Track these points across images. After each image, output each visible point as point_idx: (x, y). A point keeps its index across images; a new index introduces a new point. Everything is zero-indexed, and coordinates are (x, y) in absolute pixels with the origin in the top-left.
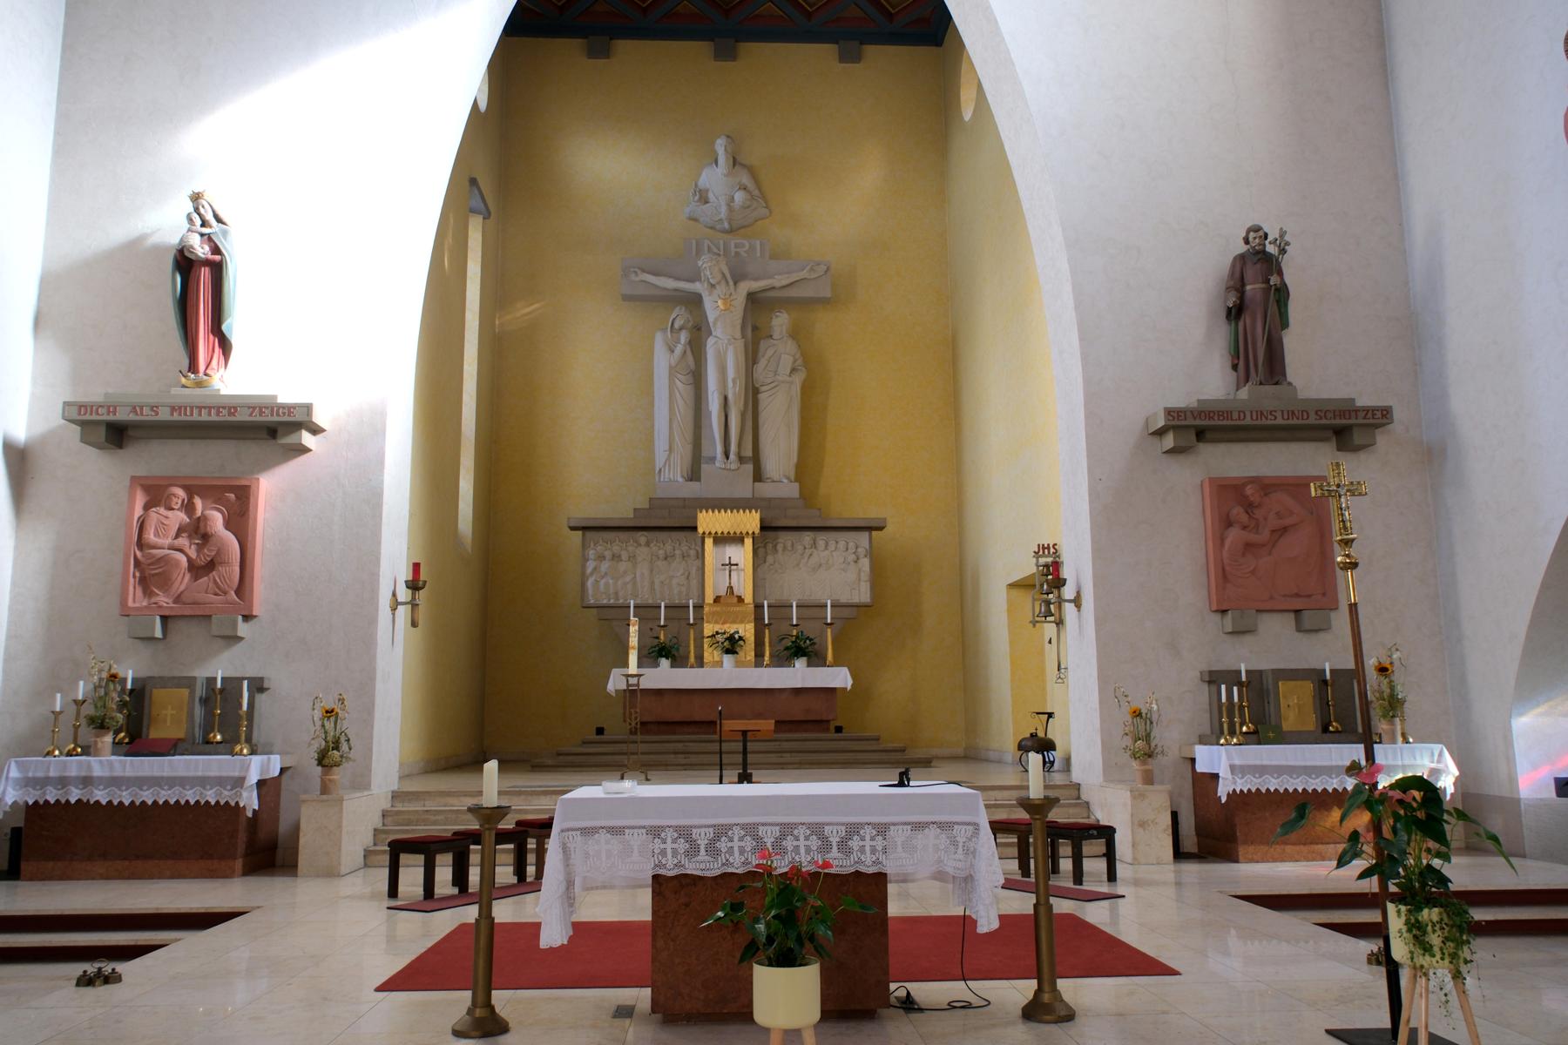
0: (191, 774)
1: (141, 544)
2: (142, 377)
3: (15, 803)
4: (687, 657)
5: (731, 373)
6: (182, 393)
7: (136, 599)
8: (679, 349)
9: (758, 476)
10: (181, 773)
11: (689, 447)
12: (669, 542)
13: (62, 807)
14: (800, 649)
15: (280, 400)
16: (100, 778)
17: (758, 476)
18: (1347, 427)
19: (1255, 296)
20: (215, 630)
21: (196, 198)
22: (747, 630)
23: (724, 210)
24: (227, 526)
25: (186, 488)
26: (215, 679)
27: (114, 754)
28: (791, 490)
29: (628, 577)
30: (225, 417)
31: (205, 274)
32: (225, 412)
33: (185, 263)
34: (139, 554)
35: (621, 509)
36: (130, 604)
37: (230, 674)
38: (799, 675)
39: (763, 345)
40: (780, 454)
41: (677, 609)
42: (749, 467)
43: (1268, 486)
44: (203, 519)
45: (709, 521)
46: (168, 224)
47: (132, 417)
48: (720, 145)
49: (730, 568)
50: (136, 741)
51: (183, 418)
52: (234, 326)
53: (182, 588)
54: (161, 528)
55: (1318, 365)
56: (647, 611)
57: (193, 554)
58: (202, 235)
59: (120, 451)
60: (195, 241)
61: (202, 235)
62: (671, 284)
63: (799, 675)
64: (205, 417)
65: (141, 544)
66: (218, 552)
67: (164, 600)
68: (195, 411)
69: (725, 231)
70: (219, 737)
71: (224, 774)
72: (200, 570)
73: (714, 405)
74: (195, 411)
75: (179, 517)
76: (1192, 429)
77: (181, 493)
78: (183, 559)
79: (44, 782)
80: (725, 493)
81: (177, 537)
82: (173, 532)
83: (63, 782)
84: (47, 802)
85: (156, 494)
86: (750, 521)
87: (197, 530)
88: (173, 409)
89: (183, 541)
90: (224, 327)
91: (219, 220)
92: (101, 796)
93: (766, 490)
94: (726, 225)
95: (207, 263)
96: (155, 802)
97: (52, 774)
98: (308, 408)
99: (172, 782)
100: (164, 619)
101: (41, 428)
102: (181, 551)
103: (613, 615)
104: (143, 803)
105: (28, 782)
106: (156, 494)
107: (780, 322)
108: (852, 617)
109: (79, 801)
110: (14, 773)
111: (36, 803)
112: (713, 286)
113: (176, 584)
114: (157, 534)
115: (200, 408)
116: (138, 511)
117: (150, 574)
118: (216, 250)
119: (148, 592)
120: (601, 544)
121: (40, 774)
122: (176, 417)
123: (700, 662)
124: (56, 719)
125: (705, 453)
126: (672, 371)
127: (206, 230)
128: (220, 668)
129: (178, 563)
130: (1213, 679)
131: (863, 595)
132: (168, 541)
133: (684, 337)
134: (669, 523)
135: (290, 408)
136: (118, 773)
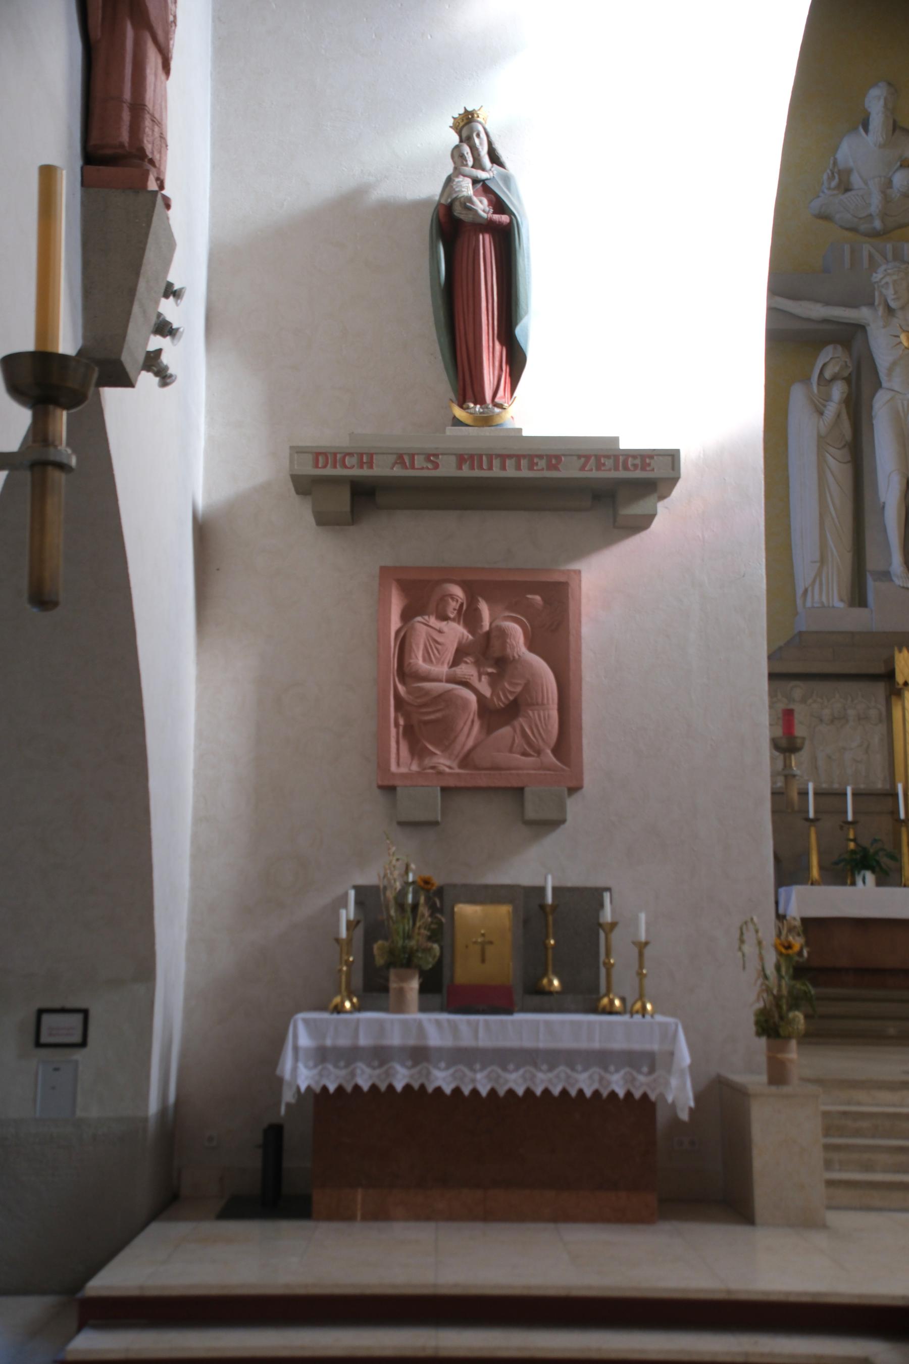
0: (583, 1045)
1: (405, 673)
2: (390, 406)
3: (309, 1088)
4: (808, 868)
6: (472, 437)
7: (401, 762)
8: (831, 409)
10: (567, 1043)
11: (848, 557)
13: (380, 1097)
15: (625, 445)
16: (440, 1050)
20: (531, 813)
21: (466, 124)
23: (876, 202)
24: (532, 646)
25: (465, 585)
26: (542, 890)
27: (423, 1009)
30: (541, 472)
31: (486, 244)
32: (542, 463)
34: (401, 688)
36: (394, 768)
37: (574, 879)
44: (498, 635)
46: (415, 162)
47: (398, 471)
51: (477, 473)
52: (534, 330)
53: (470, 743)
54: (433, 646)
57: (487, 691)
58: (475, 181)
59: (351, 528)
60: (466, 188)
61: (475, 181)
62: (817, 311)
64: (510, 472)
65: (405, 673)
66: (527, 687)
67: (444, 762)
68: (496, 463)
69: (875, 234)
70: (556, 983)
71: (637, 1046)
72: (494, 715)
74: (496, 463)
77: (458, 591)
78: (473, 698)
79: (350, 1055)
81: (455, 663)
82: (450, 656)
83: (380, 1055)
84: (357, 1088)
85: (419, 593)
87: (487, 651)
88: (461, 459)
89: (467, 670)
90: (518, 331)
91: (495, 158)
92: (442, 1079)
94: (878, 224)
95: (490, 227)
96: (529, 1092)
97: (364, 1041)
98: (673, 456)
99: (552, 1058)
100: (444, 789)
101: (225, 491)
102: (466, 684)
104: (511, 1092)
105: (322, 1055)
106: (419, 593)
109: (408, 1087)
110: (305, 1040)
111: (340, 1089)
112: (890, 311)
113: (462, 738)
114: (428, 658)
115: (503, 457)
116: (395, 622)
117: (421, 720)
118: (499, 206)
119: (417, 751)
121: (344, 1042)
122: (466, 472)
124: (641, 955)
125: (873, 562)
126: (822, 442)
127: (482, 175)
128: (541, 866)
129: (466, 702)
132: (443, 669)
133: (838, 391)
135: (645, 457)
136: (467, 1041)
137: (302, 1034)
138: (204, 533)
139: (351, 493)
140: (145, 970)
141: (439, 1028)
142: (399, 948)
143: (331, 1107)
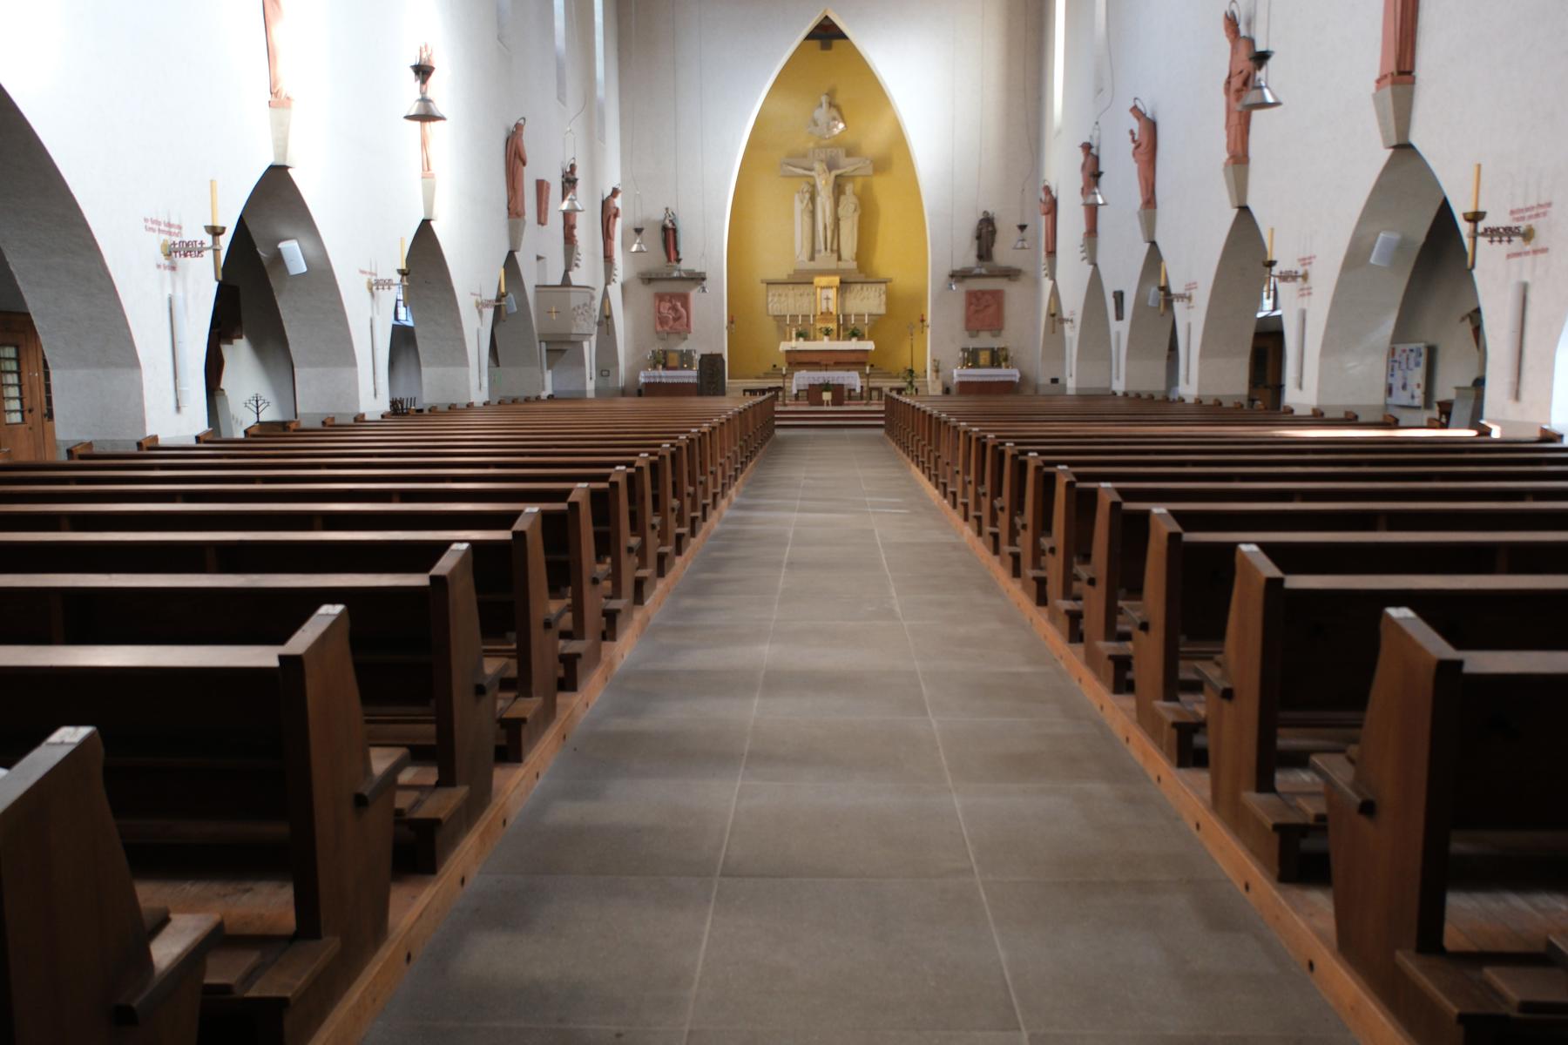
5: (828, 213)
9: (839, 258)
12: (802, 288)
14: (855, 334)
17: (839, 258)
18: (1011, 274)
19: (986, 232)
22: (833, 326)
28: (854, 265)
29: (788, 303)
33: (665, 229)
35: (782, 275)
38: (854, 344)
39: (842, 198)
40: (849, 246)
41: (806, 317)
42: (835, 256)
43: (984, 293)
45: (820, 281)
48: (824, 99)
49: (826, 297)
50: (665, 367)
55: (1004, 253)
56: (794, 317)
63: (854, 344)
72: (676, 319)
73: (820, 227)
75: (668, 305)
76: (958, 276)
80: (825, 267)
86: (836, 280)
87: (674, 308)
93: (842, 265)
103: (779, 318)
107: (849, 188)
108: (877, 320)
117: (662, 321)
120: (773, 290)
123: (815, 339)
128: (683, 347)
130: (964, 350)
131: (882, 310)
133: (807, 196)
134: (801, 280)
137: (642, 374)
138: (623, 287)
139: (648, 279)
140: (617, 364)
141: (663, 373)
142: (661, 360)
143: (647, 385)
